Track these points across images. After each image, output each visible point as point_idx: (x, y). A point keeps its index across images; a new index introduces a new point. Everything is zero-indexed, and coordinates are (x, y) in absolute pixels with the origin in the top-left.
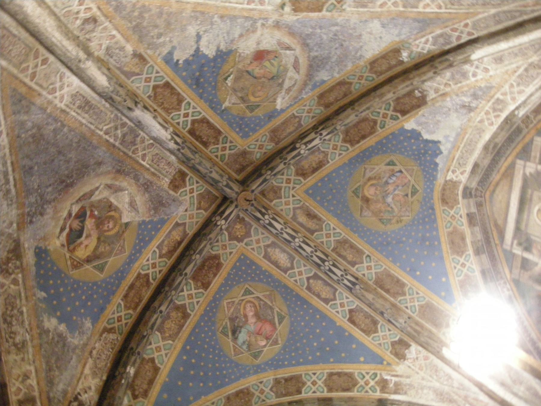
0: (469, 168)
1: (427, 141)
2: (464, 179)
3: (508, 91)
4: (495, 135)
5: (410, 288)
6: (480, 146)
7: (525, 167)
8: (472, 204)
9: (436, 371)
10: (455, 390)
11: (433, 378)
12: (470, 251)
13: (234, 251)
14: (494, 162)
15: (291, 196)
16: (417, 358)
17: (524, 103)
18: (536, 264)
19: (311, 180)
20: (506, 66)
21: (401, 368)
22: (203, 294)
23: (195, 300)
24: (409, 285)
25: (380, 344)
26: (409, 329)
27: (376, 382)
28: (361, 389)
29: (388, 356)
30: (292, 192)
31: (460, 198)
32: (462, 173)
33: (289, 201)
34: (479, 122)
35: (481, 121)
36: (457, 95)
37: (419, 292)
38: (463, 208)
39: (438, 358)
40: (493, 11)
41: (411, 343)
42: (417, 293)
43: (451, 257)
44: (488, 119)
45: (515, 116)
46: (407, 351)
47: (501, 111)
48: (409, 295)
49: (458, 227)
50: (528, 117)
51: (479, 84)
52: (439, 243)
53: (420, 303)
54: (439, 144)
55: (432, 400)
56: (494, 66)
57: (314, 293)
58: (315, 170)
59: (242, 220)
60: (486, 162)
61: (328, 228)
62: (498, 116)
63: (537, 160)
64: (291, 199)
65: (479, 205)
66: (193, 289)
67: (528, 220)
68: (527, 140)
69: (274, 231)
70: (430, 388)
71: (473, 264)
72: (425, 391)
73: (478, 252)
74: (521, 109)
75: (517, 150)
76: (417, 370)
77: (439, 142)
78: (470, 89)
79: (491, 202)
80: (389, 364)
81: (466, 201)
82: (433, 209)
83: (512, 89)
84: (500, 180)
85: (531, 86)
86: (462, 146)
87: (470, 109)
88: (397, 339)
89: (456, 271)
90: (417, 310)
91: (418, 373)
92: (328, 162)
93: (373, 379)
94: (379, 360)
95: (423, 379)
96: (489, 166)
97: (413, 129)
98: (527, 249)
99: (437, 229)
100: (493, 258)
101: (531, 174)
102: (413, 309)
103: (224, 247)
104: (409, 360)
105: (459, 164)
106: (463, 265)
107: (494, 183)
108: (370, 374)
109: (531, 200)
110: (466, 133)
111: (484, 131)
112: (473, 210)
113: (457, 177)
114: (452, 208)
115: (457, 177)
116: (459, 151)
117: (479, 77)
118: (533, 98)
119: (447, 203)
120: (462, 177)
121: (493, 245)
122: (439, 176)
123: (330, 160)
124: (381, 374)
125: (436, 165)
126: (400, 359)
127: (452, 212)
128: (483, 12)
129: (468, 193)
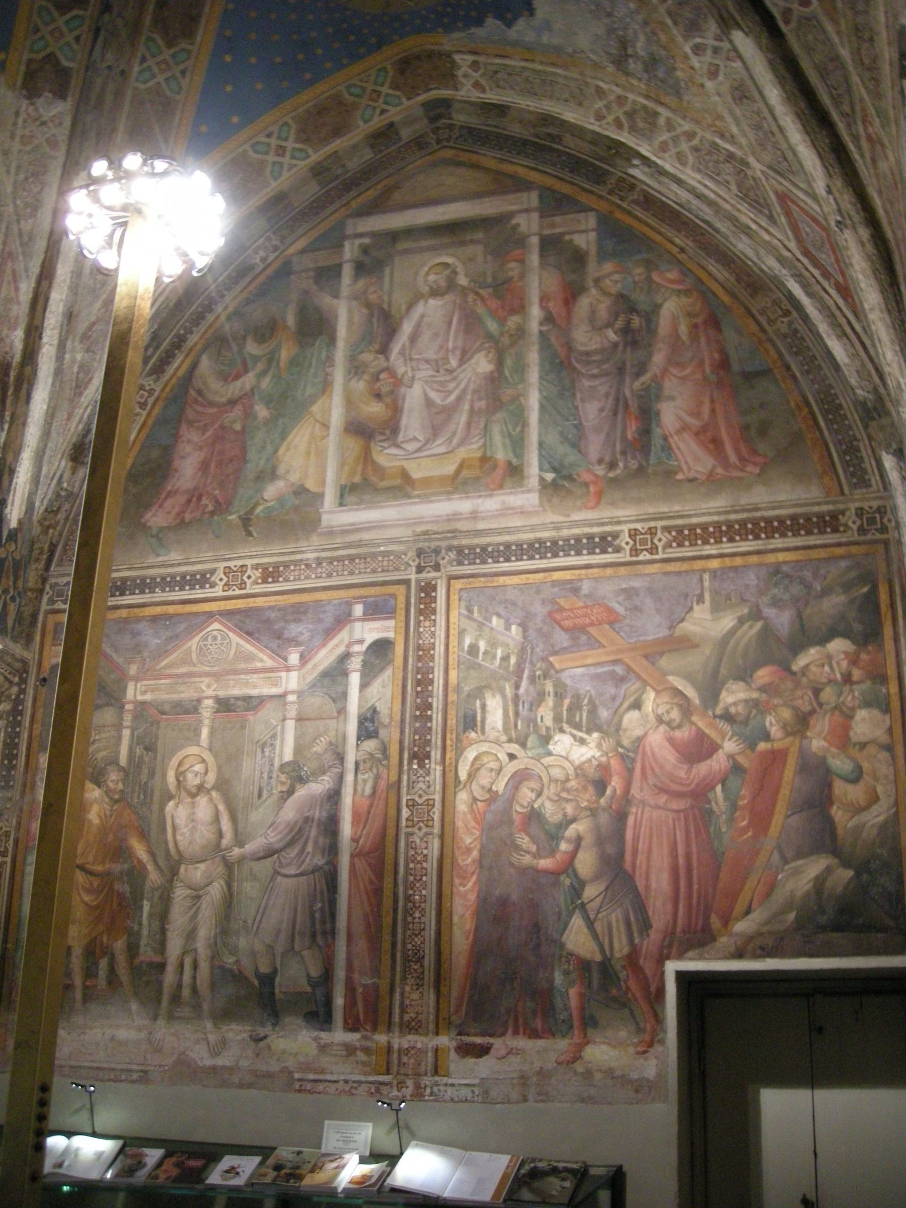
0: (492, 97)
2: (466, 92)
3: (679, 131)
4: (577, 131)
5: (189, 52)
7: (527, 211)
9: (36, 175)
11: (17, 174)
12: (315, 157)
14: (520, 146)
16: (43, 123)
17: (662, 172)
18: (336, 296)
20: (731, 113)
26: (99, 81)
31: (422, 98)
32: (477, 85)
34: (598, 87)
35: (600, 93)
36: (646, 23)
37: (188, 75)
39: (64, 166)
40: (845, 53)
41: (69, 99)
42: (183, 72)
43: (287, 119)
44: (608, 107)
45: (628, 160)
46: (50, 95)
47: (633, 129)
48: (174, 56)
50: (632, 187)
52: (311, 83)
54: (526, 13)
56: (725, 88)
60: (516, 130)
62: (619, 125)
63: (547, 232)
65: (419, 143)
67: (421, 250)
68: (584, 198)
71: (292, 169)
73: (318, 171)
74: (647, 170)
75: (557, 185)
76: (19, 133)
77: (531, 12)
78: (665, 48)
79: (434, 165)
81: (420, 112)
82: (379, 46)
83: (683, 139)
84: (487, 170)
85: (698, 176)
86: (538, 67)
87: (620, 61)
88: (66, 63)
89: (263, 139)
91: (12, 137)
96: (508, 138)
98: (360, 269)
100: (316, 207)
101: (518, 225)
104: (31, 108)
105: (496, 72)
106: (281, 151)
109: (463, 243)
111: (580, 104)
112: (406, 134)
113: (465, 76)
114: (395, 86)
115: (465, 76)
116: (523, 64)
117: (695, 62)
118: (674, 187)
119: (402, 72)
120: (468, 90)
122: (457, 35)
126: (24, 85)
127: (385, 90)
128: (839, 33)
129: (438, 110)
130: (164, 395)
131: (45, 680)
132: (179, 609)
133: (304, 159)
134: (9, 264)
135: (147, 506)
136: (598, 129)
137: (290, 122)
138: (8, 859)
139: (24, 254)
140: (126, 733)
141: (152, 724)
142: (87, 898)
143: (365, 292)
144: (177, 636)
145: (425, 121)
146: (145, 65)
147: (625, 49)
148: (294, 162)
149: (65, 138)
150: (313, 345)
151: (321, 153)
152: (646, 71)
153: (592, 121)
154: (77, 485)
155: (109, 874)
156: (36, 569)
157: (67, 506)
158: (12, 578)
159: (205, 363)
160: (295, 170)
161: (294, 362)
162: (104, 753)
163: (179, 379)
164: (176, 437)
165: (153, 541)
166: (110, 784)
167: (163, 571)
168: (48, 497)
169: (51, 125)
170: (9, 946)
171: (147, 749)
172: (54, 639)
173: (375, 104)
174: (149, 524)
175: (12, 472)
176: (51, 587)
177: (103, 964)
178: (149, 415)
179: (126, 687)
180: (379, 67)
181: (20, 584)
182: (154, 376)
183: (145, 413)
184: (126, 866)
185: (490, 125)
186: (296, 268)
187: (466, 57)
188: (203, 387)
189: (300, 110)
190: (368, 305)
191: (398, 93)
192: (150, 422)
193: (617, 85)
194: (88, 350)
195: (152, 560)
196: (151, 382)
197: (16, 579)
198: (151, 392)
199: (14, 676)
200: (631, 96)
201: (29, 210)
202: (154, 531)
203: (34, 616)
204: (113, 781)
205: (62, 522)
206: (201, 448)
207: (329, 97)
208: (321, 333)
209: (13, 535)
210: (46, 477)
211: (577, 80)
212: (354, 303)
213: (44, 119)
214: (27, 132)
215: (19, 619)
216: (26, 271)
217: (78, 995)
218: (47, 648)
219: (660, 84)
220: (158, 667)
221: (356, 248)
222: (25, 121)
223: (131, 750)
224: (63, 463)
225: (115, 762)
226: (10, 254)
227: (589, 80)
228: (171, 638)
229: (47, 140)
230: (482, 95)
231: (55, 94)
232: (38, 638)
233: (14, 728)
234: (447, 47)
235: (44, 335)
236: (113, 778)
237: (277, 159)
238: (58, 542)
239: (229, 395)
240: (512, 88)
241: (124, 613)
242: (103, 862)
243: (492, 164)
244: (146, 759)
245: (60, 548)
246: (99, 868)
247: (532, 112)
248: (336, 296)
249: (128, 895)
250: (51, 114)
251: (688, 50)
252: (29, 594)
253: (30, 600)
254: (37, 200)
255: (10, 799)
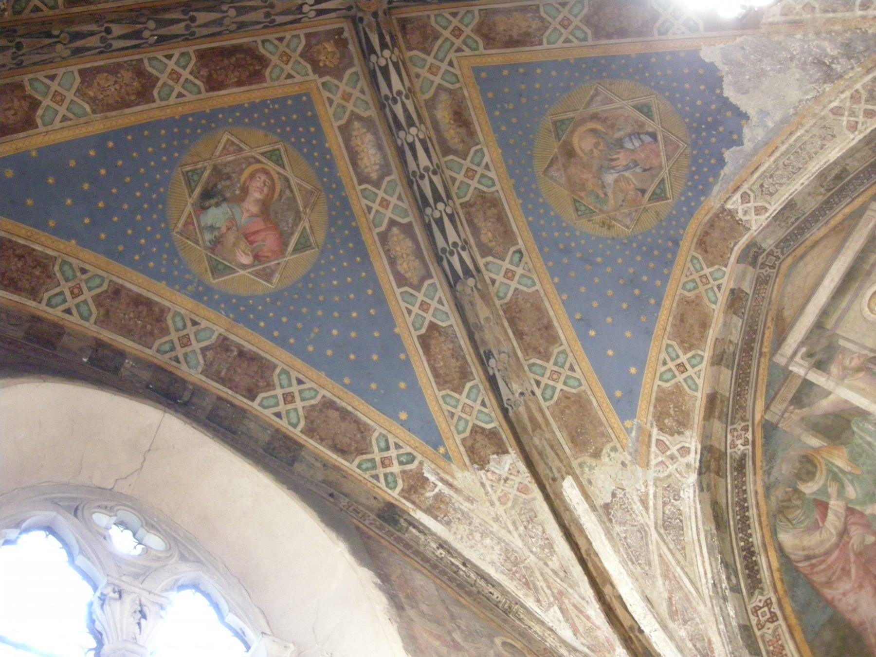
0: (775, 206)
1: (726, 103)
2: (756, 223)
4: (851, 153)
5: (564, 352)
6: (815, 167)
8: (749, 277)
9: (531, 520)
10: (547, 570)
11: (517, 529)
12: (707, 354)
13: (298, 78)
15: (447, 60)
16: (506, 480)
18: (828, 393)
19: (497, 57)
21: (466, 477)
22: (200, 92)
23: (178, 89)
24: (566, 346)
25: (452, 415)
26: (522, 409)
27: (403, 472)
28: (369, 465)
29: (455, 443)
30: (452, 55)
32: (759, 211)
33: (439, 68)
34: (832, 110)
35: (837, 112)
36: (818, 34)
37: (576, 367)
38: (729, 275)
41: (510, 450)
42: (572, 369)
43: (666, 341)
44: (852, 113)
46: (495, 456)
49: (706, 300)
51: (864, 27)
52: (658, 304)
53: (565, 388)
54: (743, 122)
55: (493, 563)
57: (387, 252)
58: (511, 43)
59: (342, 43)
60: (812, 205)
61: (477, 160)
64: (444, 66)
65: (762, 282)
66: (188, 69)
67: (847, 309)
69: (385, 90)
70: (500, 540)
72: (488, 541)
73: (718, 360)
76: (494, 498)
77: (745, 116)
78: (845, 31)
79: (788, 275)
80: (447, 457)
81: (741, 266)
82: (676, 243)
84: (826, 236)
86: (783, 148)
87: (829, 75)
88: (489, 426)
89: (663, 369)
90: (556, 397)
92: (541, 43)
93: (401, 463)
94: (434, 440)
95: (497, 519)
96: (813, 214)
97: (712, 64)
98: (821, 365)
99: (666, 279)
102: (549, 392)
103: (286, 58)
104: (489, 474)
105: (762, 186)
106: (682, 367)
107: (808, 243)
108: (401, 451)
110: (802, 125)
111: (834, 136)
112: (747, 287)
113: (745, 213)
114: (711, 264)
115: (745, 213)
116: (772, 159)
119: (706, 251)
120: (756, 220)
121: (755, 354)
122: (716, 189)
123: (545, 41)
124: (421, 463)
125: (722, 163)
126: (473, 461)
127: (707, 271)
129: (752, 255)
130: (781, 592)
133: (701, 362)
134: (566, 601)
136: (862, 136)
137: (669, 342)
139: (571, 586)
143: (845, 368)
145: (750, 268)
146: (542, 385)
147: (824, 64)
148: (697, 369)
149: (529, 479)
150: (853, 433)
151: (707, 349)
152: (849, 58)
153: (852, 136)
159: (787, 539)
160: (702, 374)
161: (853, 459)
163: (779, 570)
164: (830, 603)
169: (512, 477)
173: (710, 286)
178: (785, 619)
180: (689, 258)
182: (757, 592)
183: (781, 621)
185: (793, 223)
186: (774, 420)
187: (734, 199)
188: (806, 553)
189: (668, 329)
190: (859, 369)
191: (717, 267)
192: (793, 621)
193: (842, 92)
194: (685, 622)
196: (760, 597)
198: (768, 603)
200: (858, 86)
201: (547, 551)
206: (861, 587)
207: (678, 305)
208: (849, 421)
211: (815, 124)
212: (846, 381)
213: (504, 476)
214: (499, 494)
216: (583, 599)
219: (866, 54)
221: (802, 362)
222: (492, 486)
226: (561, 593)
227: (823, 114)
229: (518, 490)
230: (767, 214)
231: (498, 454)
234: (718, 206)
235: (643, 628)
237: (685, 375)
239: (834, 532)
240: (781, 185)
243: (824, 230)
247: (808, 185)
248: (828, 393)
250: (506, 469)
251: (859, 13)
254: (547, 539)
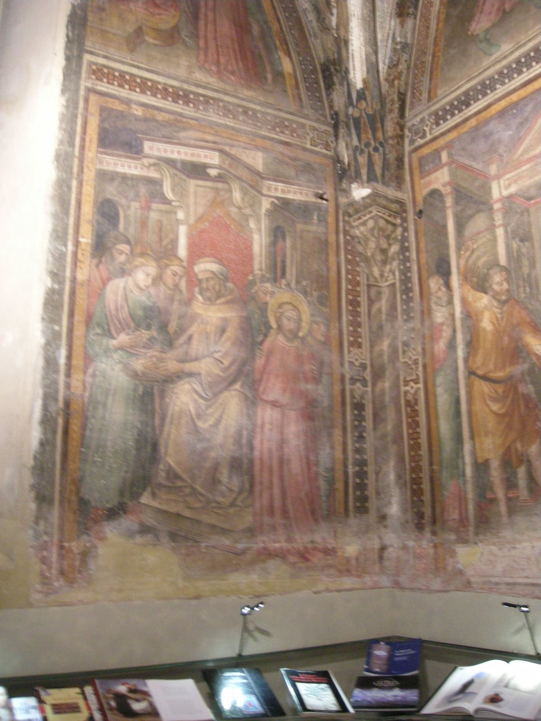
131: (421, 212)
132: (522, 93)
135: (470, 18)
138: (421, 386)
140: (500, 232)
141: (522, 214)
142: (495, 407)
144: (526, 120)
154: (409, 35)
155: (510, 378)
156: (392, 119)
157: (405, 57)
158: (370, 132)
162: (484, 259)
165: (483, 45)
166: (496, 287)
167: (498, 67)
168: (388, 56)
170: (435, 467)
171: (522, 240)
172: (421, 172)
174: (475, 33)
175: (346, 42)
176: (410, 130)
177: (521, 472)
179: (490, 188)
181: (380, 135)
184: (526, 366)
195: (486, 62)
197: (374, 130)
199: (395, 218)
202: (482, 36)
203: (400, 160)
204: (498, 283)
205: (405, 72)
209: (361, 95)
210: (382, 41)
215: (385, 166)
217: (503, 508)
218: (417, 183)
220: (516, 157)
223: (508, 247)
224: (393, 23)
225: (495, 264)
228: (521, 124)
232: (408, 178)
233: (404, 265)
236: (497, 280)
238: (406, 90)
241: (473, 122)
242: (504, 367)
244: (524, 250)
245: (409, 95)
246: (500, 375)
249: (534, 396)
252: (391, 142)
253: (393, 146)
255: (413, 329)
